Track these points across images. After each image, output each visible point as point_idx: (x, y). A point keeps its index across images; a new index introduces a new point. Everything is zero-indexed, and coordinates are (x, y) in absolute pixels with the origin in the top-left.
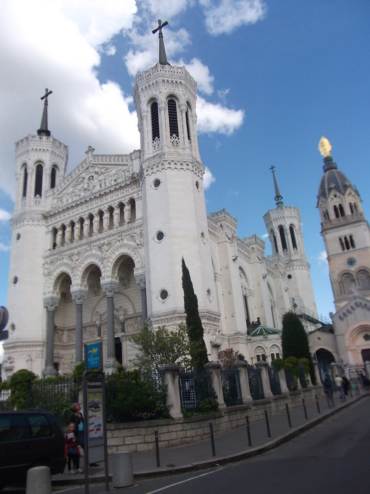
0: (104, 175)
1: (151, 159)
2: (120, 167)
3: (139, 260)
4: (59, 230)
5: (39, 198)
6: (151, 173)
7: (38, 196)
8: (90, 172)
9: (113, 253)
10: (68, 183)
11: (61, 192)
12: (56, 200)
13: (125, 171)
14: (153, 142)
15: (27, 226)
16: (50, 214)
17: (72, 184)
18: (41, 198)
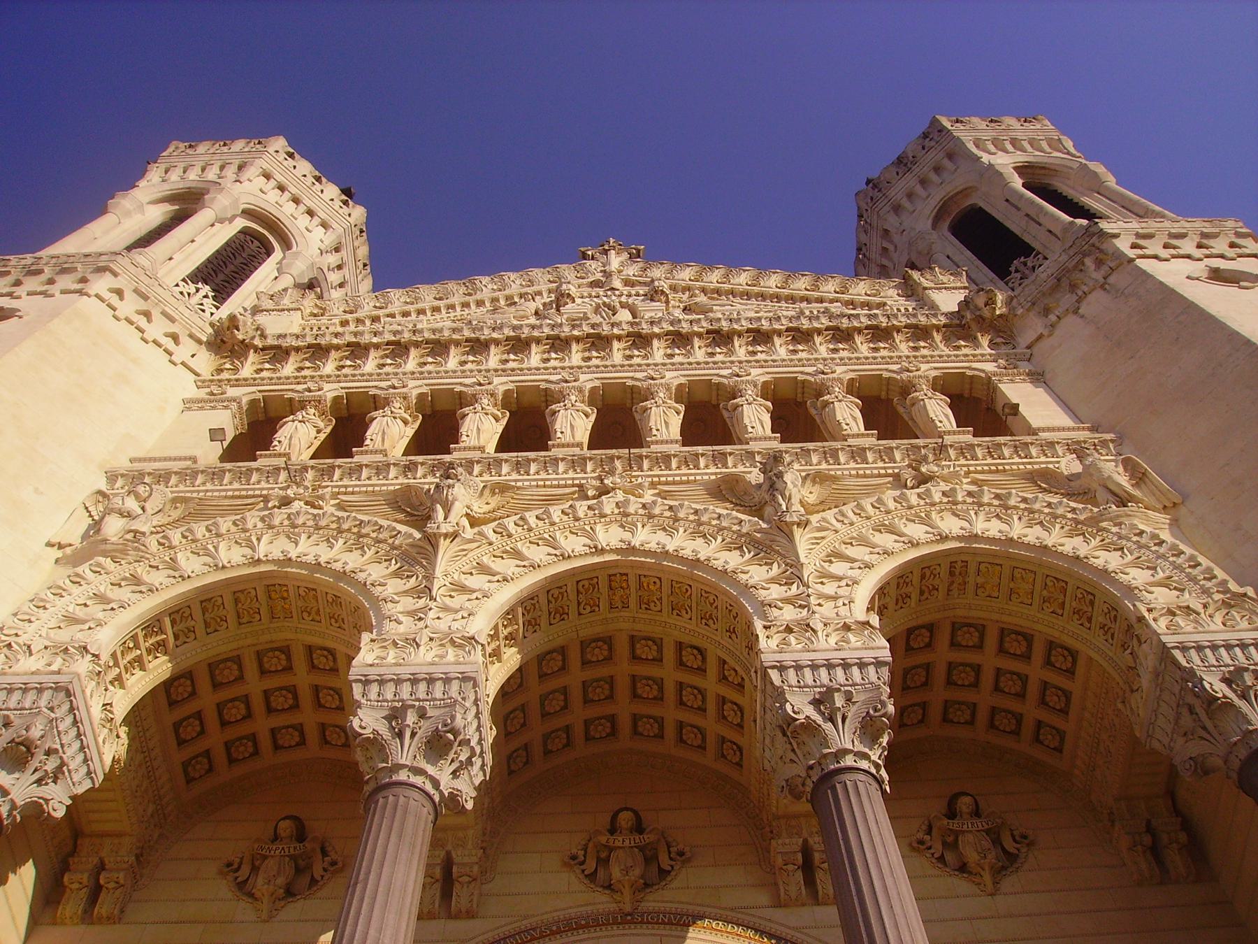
5: (206, 297)
8: (613, 289)
18: (217, 308)
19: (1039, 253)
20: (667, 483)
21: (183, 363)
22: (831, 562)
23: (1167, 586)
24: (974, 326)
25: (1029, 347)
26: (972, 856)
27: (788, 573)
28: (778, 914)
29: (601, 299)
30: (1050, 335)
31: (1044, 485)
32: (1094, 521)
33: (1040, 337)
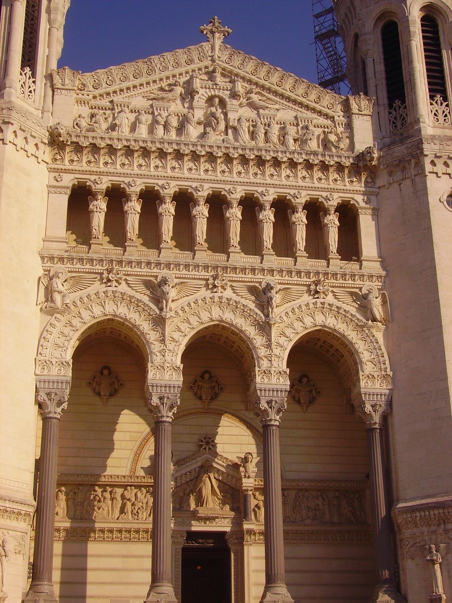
0: (261, 111)
1: (448, 143)
2: (309, 114)
3: (372, 357)
4: (100, 197)
5: (29, 78)
6: (443, 174)
7: (27, 70)
8: (216, 84)
9: (295, 317)
10: (137, 82)
11: (108, 94)
12: (86, 111)
13: (326, 130)
14: (431, 104)
15: (10, 147)
16: (74, 139)
17: (145, 89)
19: (405, 108)
20: (235, 281)
21: (42, 161)
22: (280, 337)
23: (372, 362)
24: (362, 169)
25: (379, 188)
26: (302, 401)
27: (267, 343)
28: (246, 413)
29: (210, 91)
30: (388, 188)
31: (354, 298)
32: (362, 327)
33: (384, 186)
